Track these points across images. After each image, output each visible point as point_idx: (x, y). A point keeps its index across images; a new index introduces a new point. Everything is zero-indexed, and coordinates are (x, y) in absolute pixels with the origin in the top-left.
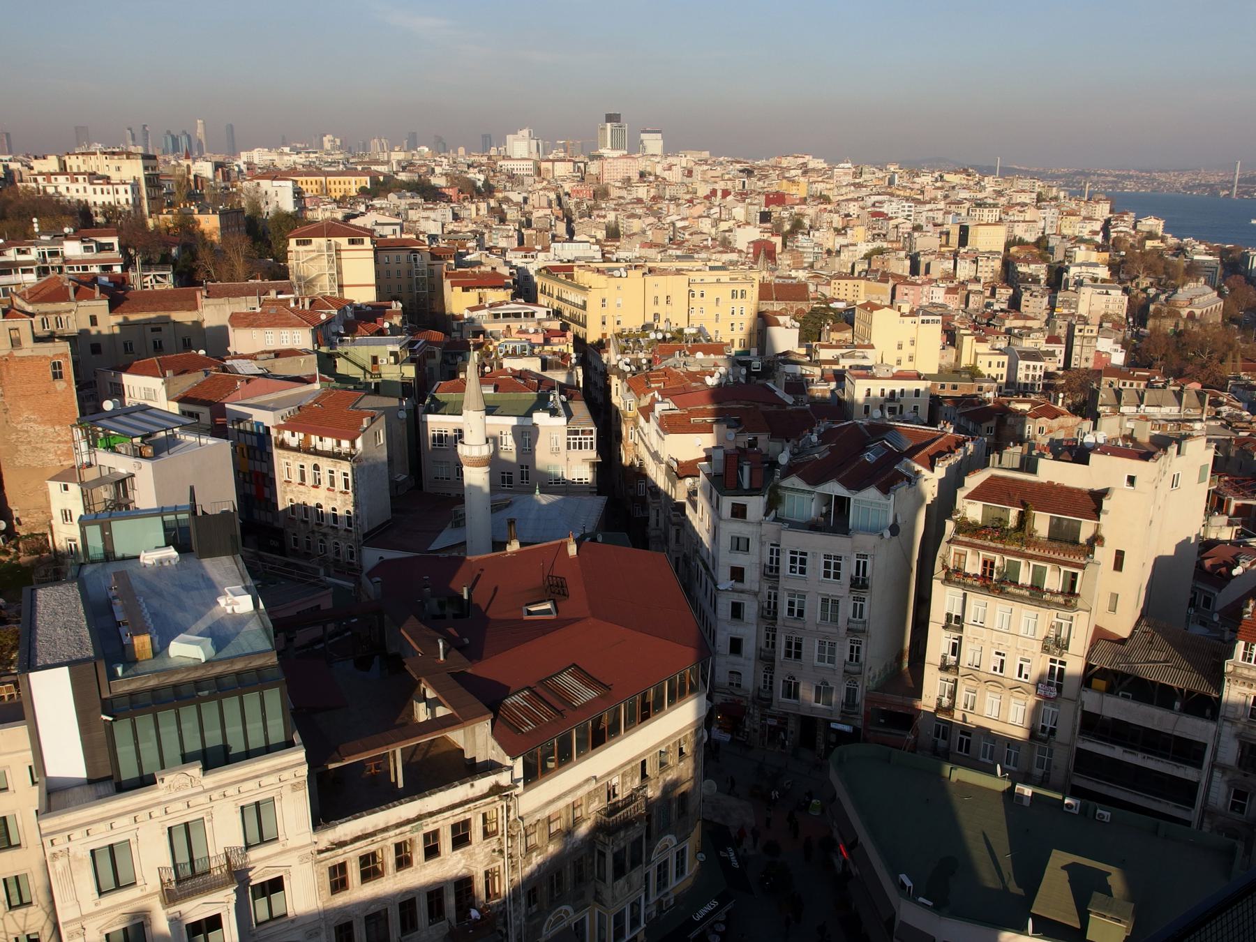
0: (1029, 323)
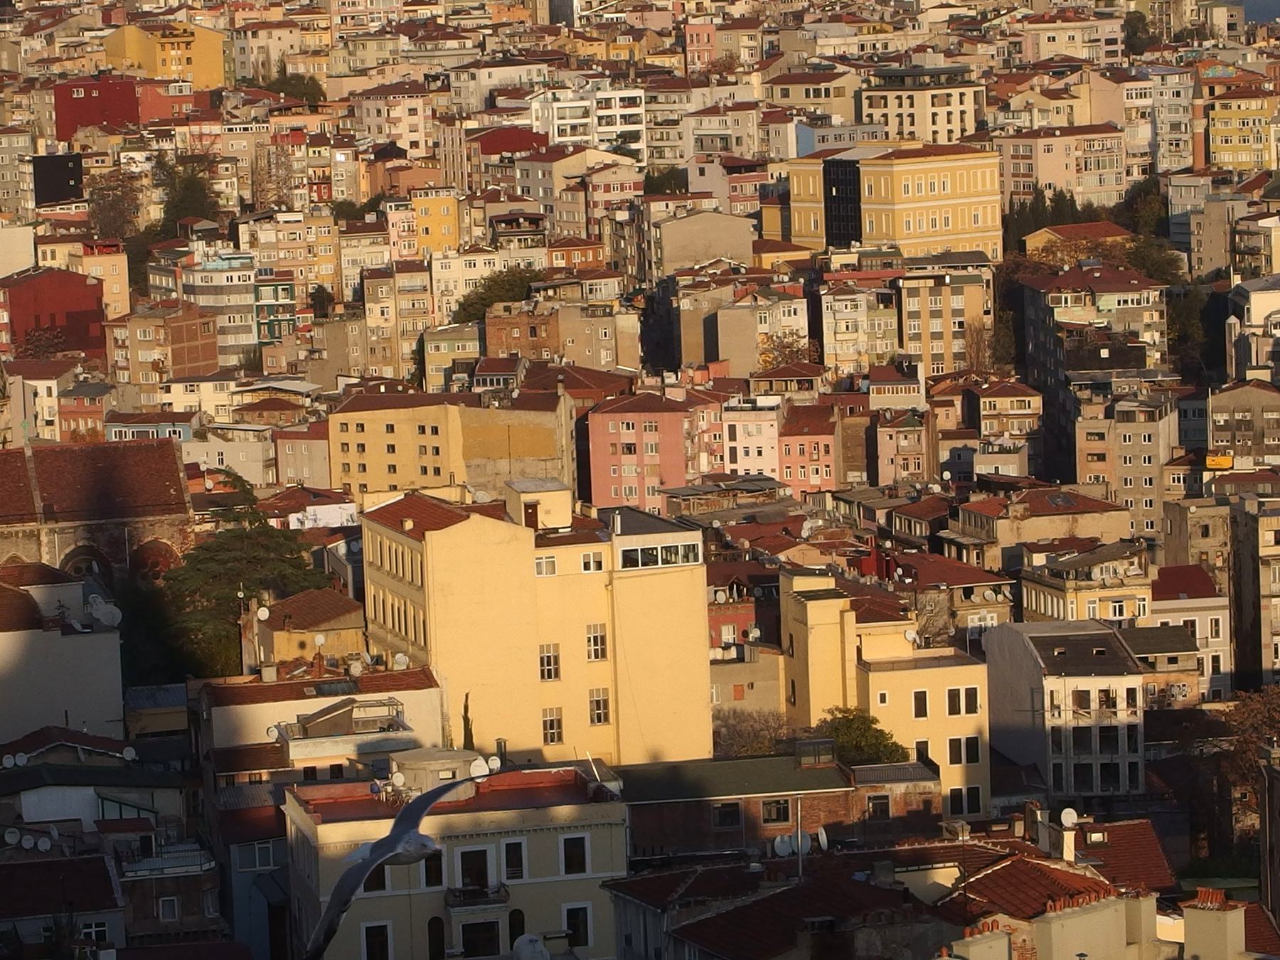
0: (1089, 526)
